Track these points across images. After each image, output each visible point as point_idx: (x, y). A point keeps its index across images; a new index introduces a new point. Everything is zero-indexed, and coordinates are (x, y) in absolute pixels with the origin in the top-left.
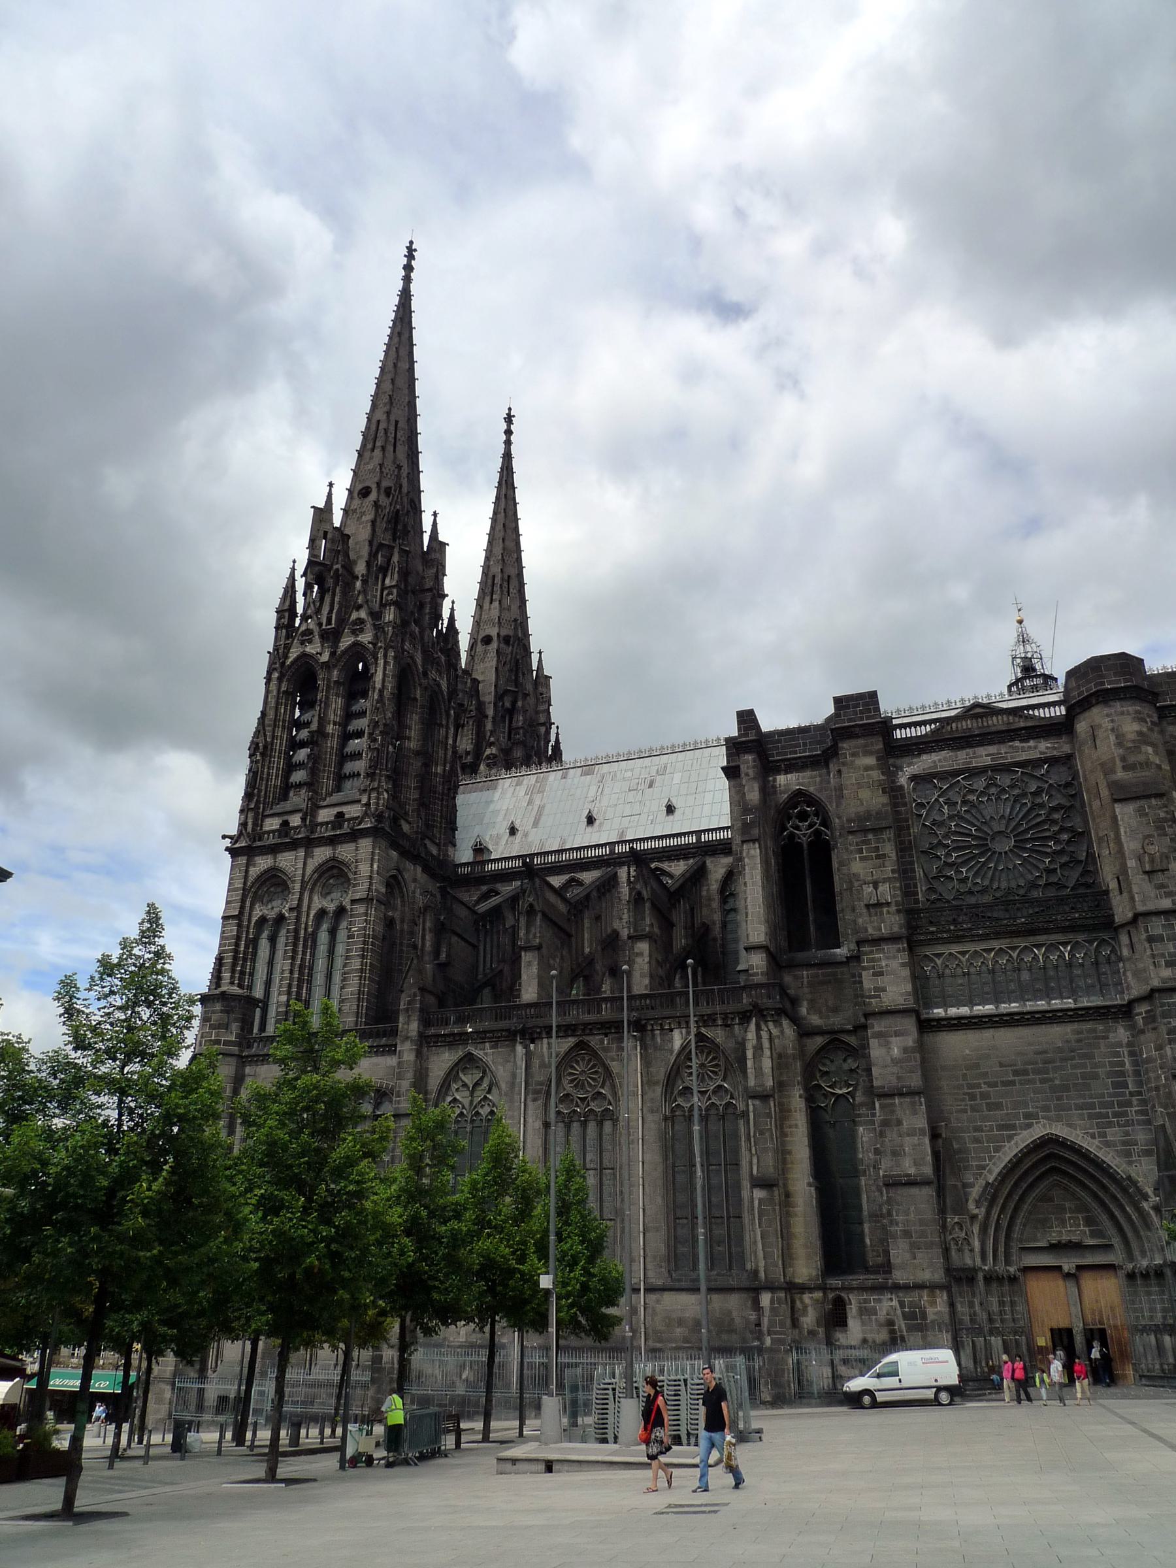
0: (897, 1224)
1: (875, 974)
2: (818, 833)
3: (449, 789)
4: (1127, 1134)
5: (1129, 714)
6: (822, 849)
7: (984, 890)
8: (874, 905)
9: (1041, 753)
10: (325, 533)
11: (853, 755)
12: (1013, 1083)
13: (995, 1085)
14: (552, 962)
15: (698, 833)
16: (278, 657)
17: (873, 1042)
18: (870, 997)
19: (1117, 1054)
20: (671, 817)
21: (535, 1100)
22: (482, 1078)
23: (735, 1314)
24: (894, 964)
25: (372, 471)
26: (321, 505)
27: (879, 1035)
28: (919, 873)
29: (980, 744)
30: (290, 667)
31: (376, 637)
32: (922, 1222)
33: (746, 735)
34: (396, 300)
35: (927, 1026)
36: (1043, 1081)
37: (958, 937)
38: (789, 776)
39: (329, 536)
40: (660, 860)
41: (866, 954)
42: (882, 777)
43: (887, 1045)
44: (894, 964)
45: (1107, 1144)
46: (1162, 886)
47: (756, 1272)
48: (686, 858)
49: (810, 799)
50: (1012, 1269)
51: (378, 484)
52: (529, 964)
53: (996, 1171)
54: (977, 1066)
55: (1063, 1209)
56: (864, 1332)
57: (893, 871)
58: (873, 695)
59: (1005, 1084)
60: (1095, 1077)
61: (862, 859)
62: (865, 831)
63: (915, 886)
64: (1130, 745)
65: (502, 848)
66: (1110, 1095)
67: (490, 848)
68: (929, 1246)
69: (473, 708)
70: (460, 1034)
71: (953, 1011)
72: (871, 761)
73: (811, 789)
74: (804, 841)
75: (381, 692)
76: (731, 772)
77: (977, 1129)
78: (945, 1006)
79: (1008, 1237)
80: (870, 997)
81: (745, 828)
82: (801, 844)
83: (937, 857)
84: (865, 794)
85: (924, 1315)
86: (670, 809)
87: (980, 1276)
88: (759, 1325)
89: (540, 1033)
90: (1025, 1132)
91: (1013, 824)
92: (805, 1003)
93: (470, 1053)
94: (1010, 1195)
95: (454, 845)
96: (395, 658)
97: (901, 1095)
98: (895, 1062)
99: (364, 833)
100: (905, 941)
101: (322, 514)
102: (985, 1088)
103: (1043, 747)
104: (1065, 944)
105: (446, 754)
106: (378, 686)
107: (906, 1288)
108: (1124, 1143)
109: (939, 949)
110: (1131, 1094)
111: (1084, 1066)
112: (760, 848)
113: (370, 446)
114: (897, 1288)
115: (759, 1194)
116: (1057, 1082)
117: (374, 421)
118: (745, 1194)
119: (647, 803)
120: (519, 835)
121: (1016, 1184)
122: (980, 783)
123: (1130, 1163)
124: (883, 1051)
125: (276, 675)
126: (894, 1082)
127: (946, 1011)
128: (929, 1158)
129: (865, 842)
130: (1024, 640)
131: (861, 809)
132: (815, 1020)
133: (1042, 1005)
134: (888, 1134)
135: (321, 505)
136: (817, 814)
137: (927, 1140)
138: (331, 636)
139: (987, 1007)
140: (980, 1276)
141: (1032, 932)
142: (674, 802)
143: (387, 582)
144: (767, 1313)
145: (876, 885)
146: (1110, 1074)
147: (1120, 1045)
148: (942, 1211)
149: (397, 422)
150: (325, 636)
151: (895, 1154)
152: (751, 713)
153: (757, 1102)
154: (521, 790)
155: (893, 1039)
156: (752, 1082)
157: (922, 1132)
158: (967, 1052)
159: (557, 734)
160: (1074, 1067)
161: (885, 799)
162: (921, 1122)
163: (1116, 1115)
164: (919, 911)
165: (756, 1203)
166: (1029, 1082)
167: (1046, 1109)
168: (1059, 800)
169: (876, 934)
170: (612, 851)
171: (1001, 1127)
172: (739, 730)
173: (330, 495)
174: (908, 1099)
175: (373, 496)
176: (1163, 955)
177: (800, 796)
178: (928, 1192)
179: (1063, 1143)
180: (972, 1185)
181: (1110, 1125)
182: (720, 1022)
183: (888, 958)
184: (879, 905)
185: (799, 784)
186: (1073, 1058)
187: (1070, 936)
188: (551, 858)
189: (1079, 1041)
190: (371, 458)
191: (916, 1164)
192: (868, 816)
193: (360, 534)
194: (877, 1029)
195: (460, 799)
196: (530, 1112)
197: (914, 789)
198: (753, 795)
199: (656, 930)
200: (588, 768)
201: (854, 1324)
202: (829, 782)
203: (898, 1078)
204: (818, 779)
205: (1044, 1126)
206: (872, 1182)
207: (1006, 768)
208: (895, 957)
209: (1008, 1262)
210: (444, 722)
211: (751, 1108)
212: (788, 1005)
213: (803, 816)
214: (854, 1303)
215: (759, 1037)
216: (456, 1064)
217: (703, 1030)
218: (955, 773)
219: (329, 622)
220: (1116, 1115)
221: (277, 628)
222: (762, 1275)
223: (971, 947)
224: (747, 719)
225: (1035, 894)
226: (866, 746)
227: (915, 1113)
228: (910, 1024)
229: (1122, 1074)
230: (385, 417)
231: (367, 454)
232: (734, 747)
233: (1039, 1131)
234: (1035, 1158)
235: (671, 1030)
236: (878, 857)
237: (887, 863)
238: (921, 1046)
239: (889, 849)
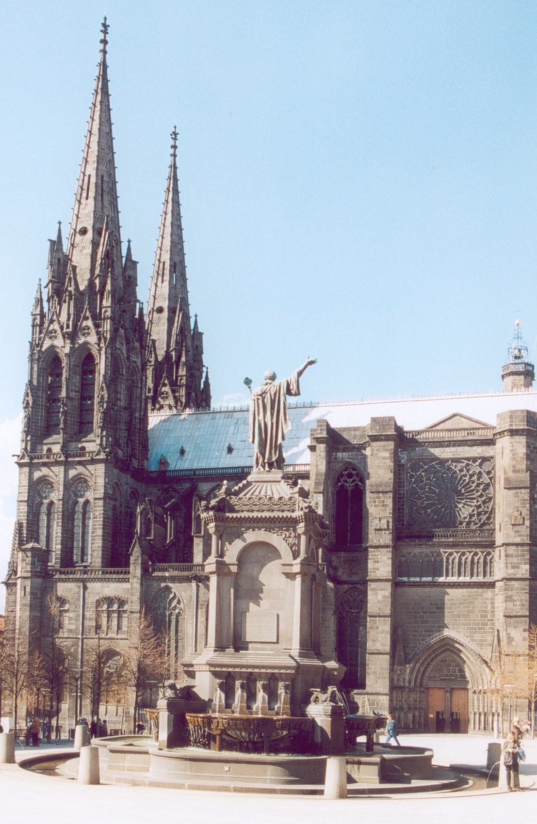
2: (357, 485)
6: (359, 494)
8: (378, 530)
10: (59, 260)
16: (33, 345)
19: (486, 603)
25: (88, 215)
26: (55, 238)
31: (99, 339)
39: (62, 262)
51: (93, 227)
61: (375, 506)
71: (412, 579)
74: (350, 489)
75: (104, 376)
78: (409, 576)
96: (111, 354)
101: (56, 245)
106: (103, 372)
113: (84, 195)
135: (54, 238)
136: (357, 475)
138: (72, 337)
143: (104, 303)
145: (380, 520)
146: (479, 612)
147: (487, 599)
149: (102, 177)
173: (60, 231)
184: (380, 530)
190: (86, 205)
193: (81, 260)
213: (350, 476)
219: (68, 327)
221: (33, 326)
229: (486, 612)
231: (83, 201)
239: (389, 502)
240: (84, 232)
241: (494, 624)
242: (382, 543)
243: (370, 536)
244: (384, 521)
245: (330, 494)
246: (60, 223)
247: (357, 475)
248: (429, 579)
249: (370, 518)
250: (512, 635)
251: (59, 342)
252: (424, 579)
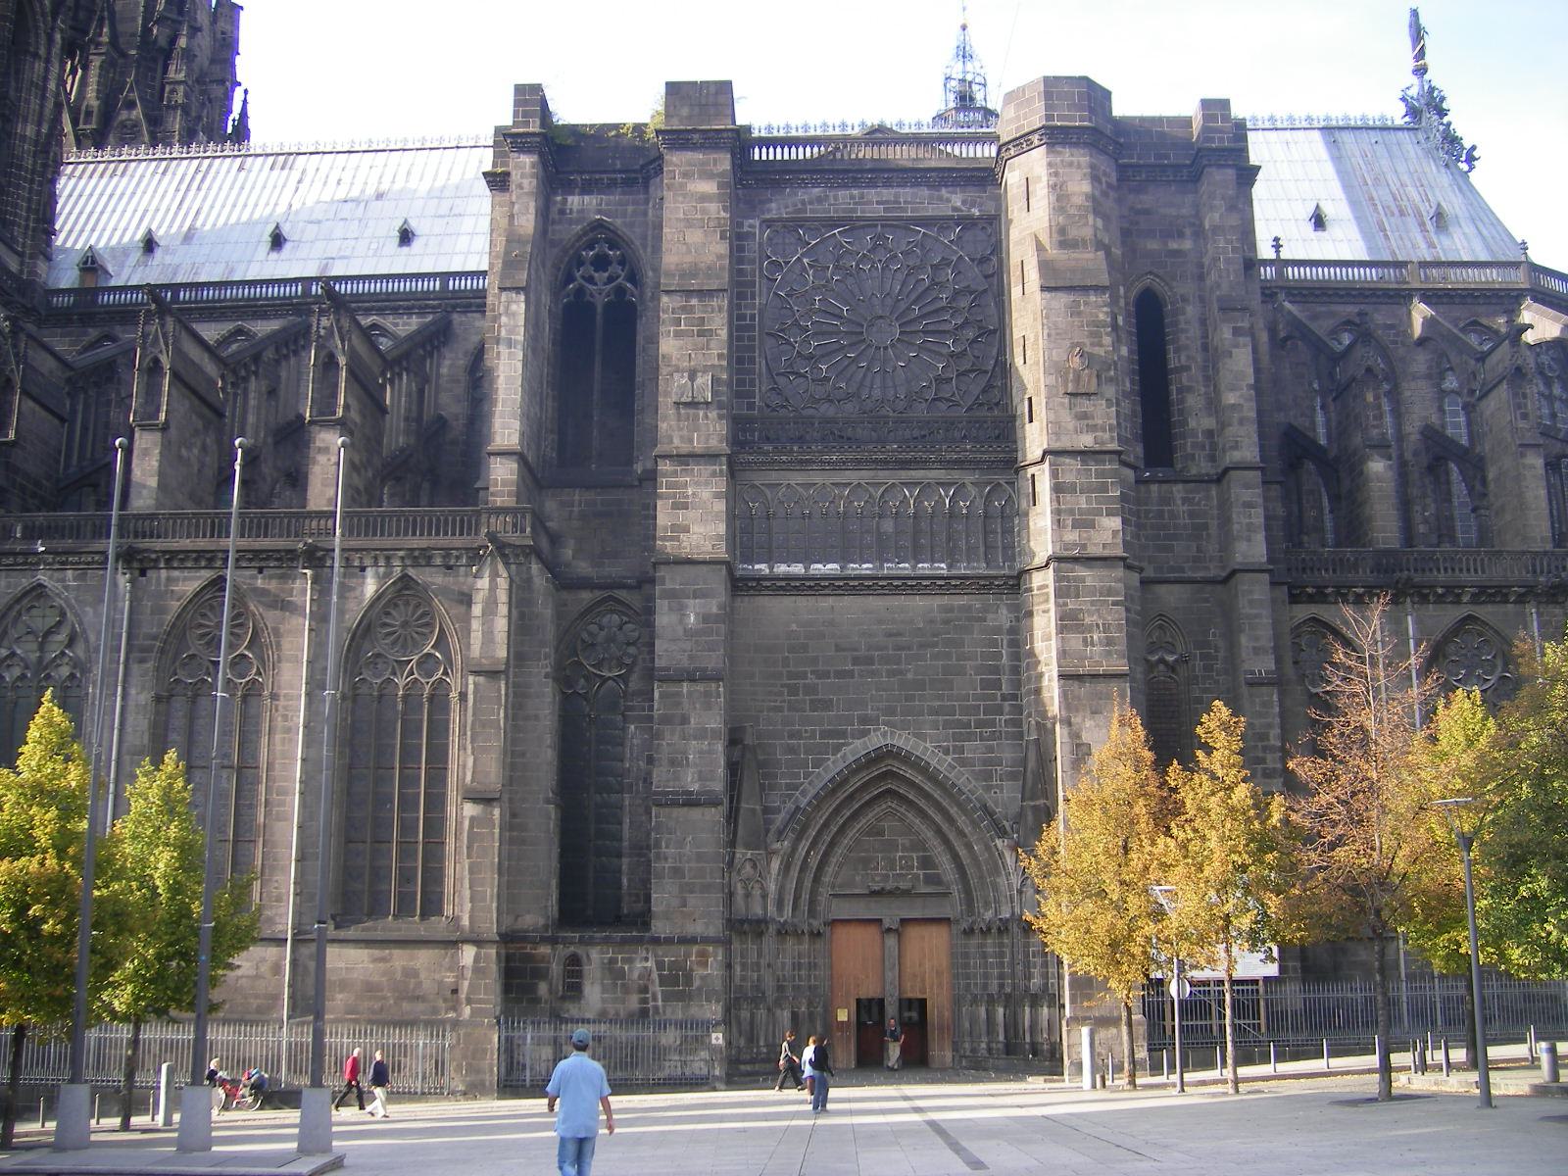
0: (666, 859)
1: (676, 506)
2: (620, 291)
3: (45, 166)
4: (991, 750)
5: (1079, 166)
7: (849, 397)
8: (686, 404)
9: (955, 209)
11: (685, 175)
12: (851, 674)
13: (826, 675)
14: (184, 452)
15: (445, 276)
17: (662, 605)
18: (664, 539)
19: (994, 644)
20: (405, 249)
21: (142, 661)
22: (59, 623)
23: (423, 976)
24: (706, 494)
27: (672, 595)
28: (760, 365)
29: (872, 184)
32: (700, 857)
33: (527, 124)
35: (741, 586)
36: (891, 674)
37: (801, 462)
38: (587, 198)
40: (381, 311)
41: (665, 475)
42: (723, 214)
43: (681, 610)
44: (706, 494)
45: (963, 762)
46: (1084, 416)
47: (456, 919)
48: (421, 314)
49: (614, 240)
50: (815, 923)
52: (146, 452)
53: (812, 792)
54: (805, 648)
55: (892, 846)
56: (604, 1001)
57: (720, 356)
58: (725, 88)
59: (840, 674)
60: (961, 672)
61: (678, 334)
62: (689, 293)
63: (752, 383)
64: (1073, 211)
65: (128, 273)
66: (977, 698)
67: (110, 269)
68: (706, 888)
69: (105, 39)
70: (26, 554)
71: (782, 569)
72: (709, 187)
73: (619, 222)
74: (600, 301)
76: (497, 181)
77: (791, 736)
78: (770, 560)
79: (817, 879)
80: (664, 539)
81: (509, 264)
82: (591, 306)
83: (788, 343)
84: (695, 236)
85: (689, 979)
86: (406, 237)
87: (772, 929)
88: (455, 991)
89: (156, 560)
90: (858, 742)
91: (903, 306)
92: (572, 542)
93: (41, 586)
94: (826, 825)
95: (49, 258)
97: (692, 680)
98: (689, 633)
100: (724, 459)
102: (811, 679)
103: (955, 200)
104: (946, 485)
105: (42, 106)
107: (669, 941)
108: (986, 762)
109: (773, 477)
110: (1004, 698)
111: (948, 656)
112: (527, 302)
114: (656, 941)
115: (470, 809)
116: (910, 676)
118: (451, 810)
119: (371, 223)
120: (158, 253)
121: (837, 811)
123: (988, 788)
124: (674, 618)
126: (685, 663)
127: (771, 568)
128: (721, 771)
129: (684, 309)
130: (964, 54)
131: (688, 259)
132: (584, 568)
133: (905, 568)
134: (667, 735)
136: (622, 262)
137: (720, 747)
139: (829, 566)
140: (772, 929)
141: (904, 465)
142: (413, 224)
144: (468, 974)
145: (692, 377)
146: (979, 670)
147: (998, 630)
148: (732, 843)
151: (673, 763)
152: (537, 89)
153: (481, 679)
154: (170, 183)
155: (691, 602)
156: (476, 650)
157: (715, 734)
158: (794, 627)
159: (245, 102)
160: (935, 657)
161: (723, 248)
162: (715, 722)
163: (980, 724)
164: (751, 420)
165: (467, 823)
166: (873, 674)
167: (891, 711)
169: (685, 449)
170: (307, 292)
171: (825, 734)
172: (516, 114)
174: (700, 687)
176: (1071, 512)
177: (599, 232)
178: (715, 815)
179: (905, 758)
180: (778, 810)
181: (970, 737)
182: (438, 561)
183: (697, 484)
184: (693, 404)
185: (599, 212)
186: (935, 645)
187: (956, 475)
188: (209, 294)
189: (947, 622)
191: (701, 778)
192: (693, 271)
194: (669, 585)
195: (64, 186)
196: (135, 680)
197: (770, 239)
198: (527, 223)
199: (355, 415)
200: (285, 157)
201: (593, 994)
202: (645, 214)
203: (691, 657)
204: (630, 208)
205: (884, 735)
206: (639, 801)
207: (906, 224)
208: (707, 484)
209: (812, 913)
210: (42, 52)
211: (471, 687)
212: (544, 543)
213: (602, 262)
214: (595, 957)
215: (493, 587)
216: (18, 600)
217: (411, 572)
218: (833, 223)
220: (980, 724)
222: (466, 921)
223: (818, 478)
224: (531, 98)
225: (920, 411)
226: (703, 164)
227: (708, 707)
228: (718, 581)
229: (996, 670)
232: (508, 140)
233: (876, 740)
234: (865, 776)
235: (363, 569)
236: (701, 334)
237: (713, 344)
238: (729, 615)
239: (719, 325)
241: (1019, 710)
242: (698, 445)
243: (663, 426)
244: (704, 380)
245: (545, 315)
247: (622, 262)
248: (832, 568)
249: (664, 371)
250: (1085, 737)
252: (818, 568)
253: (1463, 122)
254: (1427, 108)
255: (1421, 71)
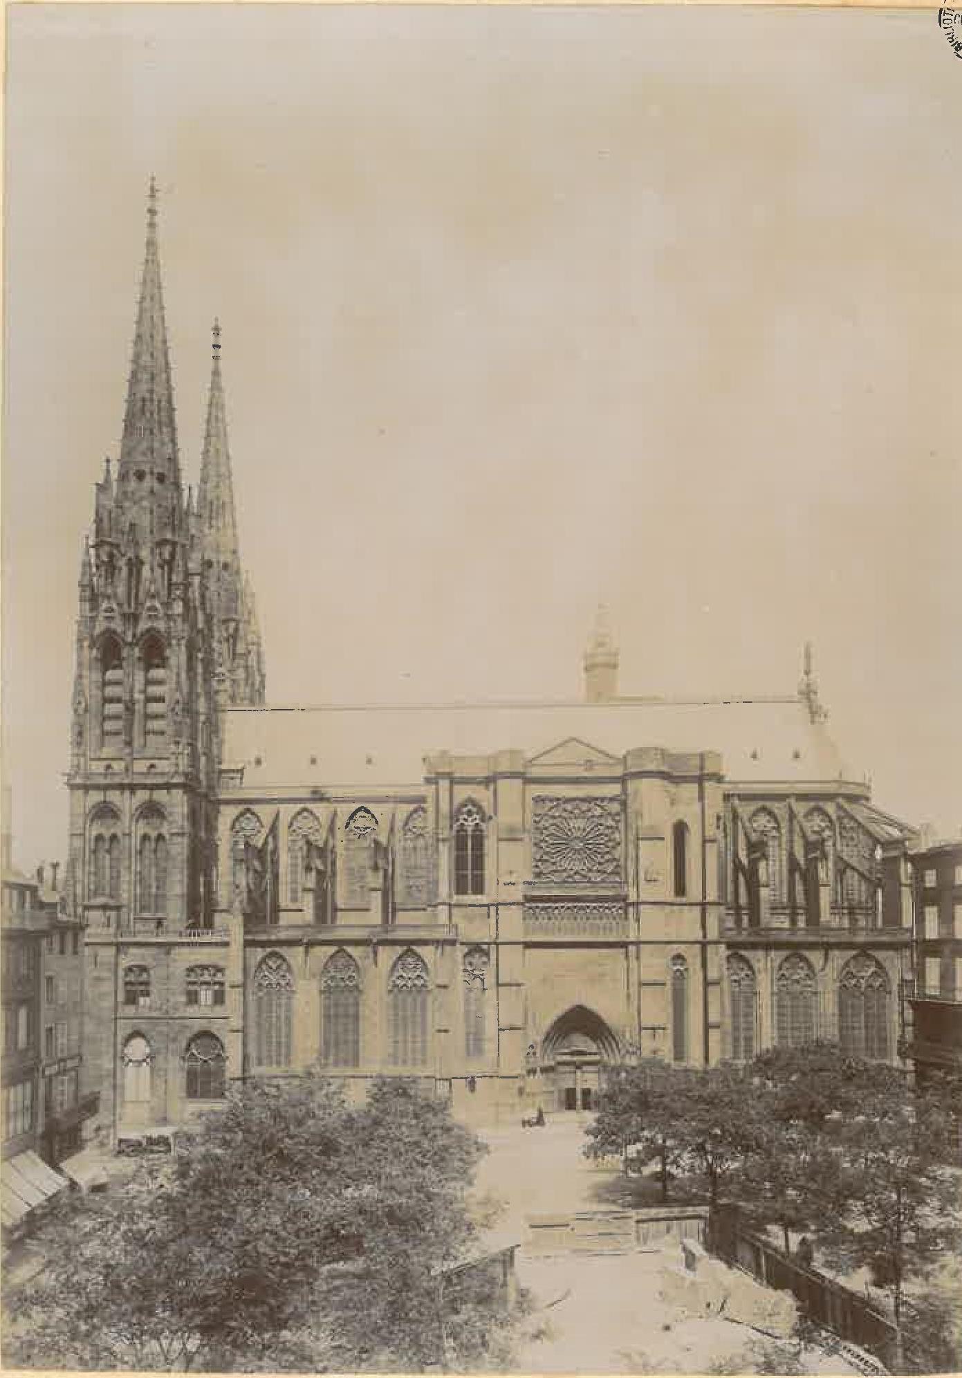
30: (98, 636)
34: (142, 253)
99: (176, 786)
117: (139, 396)
122: (569, 807)
125: (86, 644)
149: (160, 401)
150: (126, 617)
168: (610, 823)
173: (108, 471)
175: (149, 482)
193: (141, 516)
230: (147, 396)
240: (140, 476)
246: (108, 461)
251: (117, 625)
253: (821, 699)
254: (808, 694)
255: (807, 673)
